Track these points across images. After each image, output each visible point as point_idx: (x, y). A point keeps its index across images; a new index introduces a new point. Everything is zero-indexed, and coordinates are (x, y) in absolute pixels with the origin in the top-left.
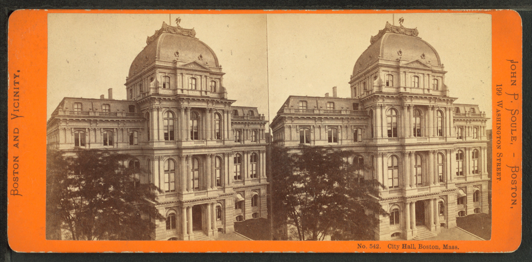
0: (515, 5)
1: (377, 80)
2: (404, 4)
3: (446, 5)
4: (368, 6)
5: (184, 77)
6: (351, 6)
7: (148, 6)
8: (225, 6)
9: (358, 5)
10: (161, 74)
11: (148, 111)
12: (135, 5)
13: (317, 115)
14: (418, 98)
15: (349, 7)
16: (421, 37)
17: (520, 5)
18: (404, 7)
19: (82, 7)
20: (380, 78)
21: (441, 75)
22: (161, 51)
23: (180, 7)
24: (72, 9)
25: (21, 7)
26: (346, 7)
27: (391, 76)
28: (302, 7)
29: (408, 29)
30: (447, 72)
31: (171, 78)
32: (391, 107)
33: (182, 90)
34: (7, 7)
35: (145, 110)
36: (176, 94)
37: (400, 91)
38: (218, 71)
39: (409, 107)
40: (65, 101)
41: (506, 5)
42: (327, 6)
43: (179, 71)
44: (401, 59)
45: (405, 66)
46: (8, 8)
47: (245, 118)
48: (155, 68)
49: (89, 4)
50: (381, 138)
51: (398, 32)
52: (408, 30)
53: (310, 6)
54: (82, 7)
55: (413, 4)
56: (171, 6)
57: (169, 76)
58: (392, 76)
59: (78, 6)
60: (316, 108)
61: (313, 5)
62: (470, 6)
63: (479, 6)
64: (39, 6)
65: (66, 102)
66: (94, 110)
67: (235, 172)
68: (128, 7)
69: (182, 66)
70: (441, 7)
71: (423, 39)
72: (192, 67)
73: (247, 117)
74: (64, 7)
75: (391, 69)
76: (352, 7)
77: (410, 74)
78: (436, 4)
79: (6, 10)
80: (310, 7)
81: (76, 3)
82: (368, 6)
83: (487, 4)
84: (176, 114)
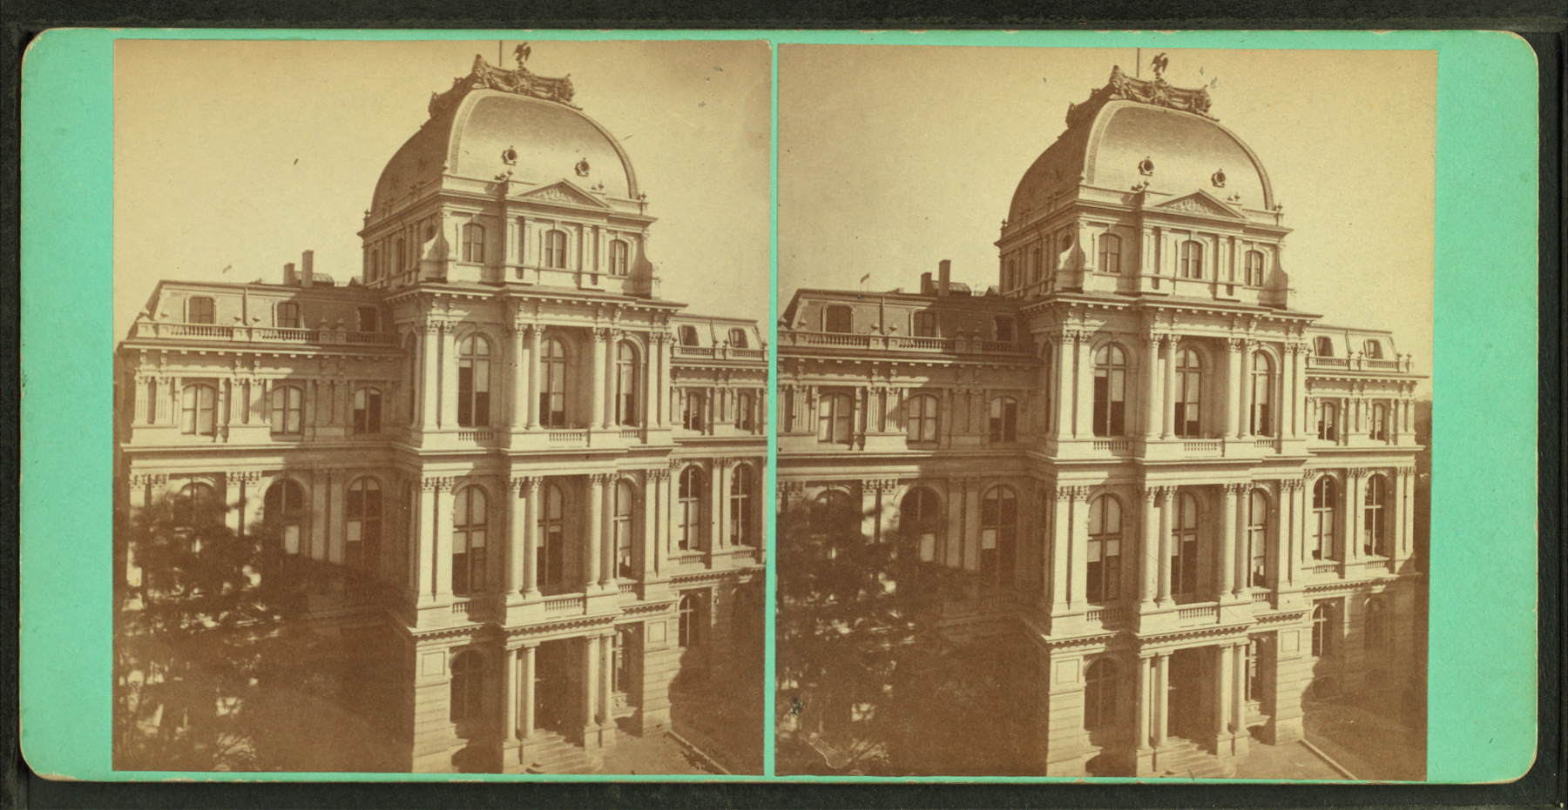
0: (1493, 15)
1: (432, 242)
2: (1169, 12)
3: (1292, 16)
5: (527, 229)
8: (649, 20)
10: (457, 219)
11: (415, 331)
12: (389, 17)
13: (877, 354)
14: (1193, 314)
15: (1011, 22)
16: (1216, 117)
17: (1508, 16)
18: (1170, 20)
19: (234, 22)
20: (1078, 244)
21: (1273, 240)
22: (463, 145)
23: (518, 20)
24: (203, 27)
27: (479, 230)
28: (874, 21)
29: (1176, 89)
30: (1292, 230)
31: (488, 232)
32: (1109, 339)
33: (520, 271)
34: (15, 20)
35: (406, 324)
36: (1136, 291)
37: (503, 277)
38: (1271, 222)
39: (1164, 343)
40: (801, 299)
41: (1464, 16)
43: (1148, 224)
44: (1148, 189)
45: (524, 199)
47: (719, 356)
48: (440, 199)
50: (657, 426)
51: (1148, 100)
52: (1177, 92)
53: (897, 18)
57: (1117, 233)
58: (1120, 239)
60: (877, 333)
63: (1388, 17)
65: (166, 293)
66: (249, 320)
67: (680, 526)
69: (522, 195)
71: (1223, 123)
72: (552, 196)
73: (724, 351)
74: (183, 22)
75: (1112, 221)
76: (1017, 20)
77: (1173, 236)
78: (1263, 13)
79: (14, 31)
81: (216, 10)
82: (1064, 18)
83: (1411, 12)
84: (1132, 351)
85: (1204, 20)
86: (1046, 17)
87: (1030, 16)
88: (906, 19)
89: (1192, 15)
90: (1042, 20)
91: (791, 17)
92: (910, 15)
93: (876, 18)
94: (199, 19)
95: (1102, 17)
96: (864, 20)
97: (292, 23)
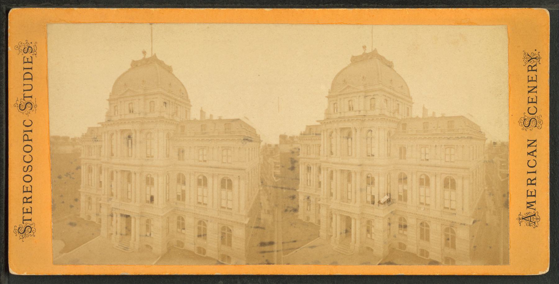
3: (467, 4)
4: (384, 5)
6: (367, 5)
7: (153, 4)
8: (234, 5)
9: (374, 3)
17: (545, 4)
19: (84, 5)
25: (19, 5)
26: (361, 5)
28: (315, 5)
34: (5, 4)
41: (529, 4)
42: (342, 5)
46: (6, 6)
49: (91, 2)
54: (84, 5)
55: (432, 3)
56: (177, 4)
59: (79, 4)
61: (327, 3)
62: (491, 5)
63: (501, 5)
64: (39, 4)
68: (132, 5)
70: (461, 5)
74: (65, 5)
78: (456, 3)
79: (4, 8)
80: (323, 6)
85: (435, 5)
86: (377, 4)
87: (372, 4)
88: (327, 5)
89: (430, 3)
90: (376, 5)
91: (286, 4)
92: (329, 3)
93: (316, 4)
94: (71, 4)
95: (398, 4)
96: (312, 5)
97: (105, 6)
